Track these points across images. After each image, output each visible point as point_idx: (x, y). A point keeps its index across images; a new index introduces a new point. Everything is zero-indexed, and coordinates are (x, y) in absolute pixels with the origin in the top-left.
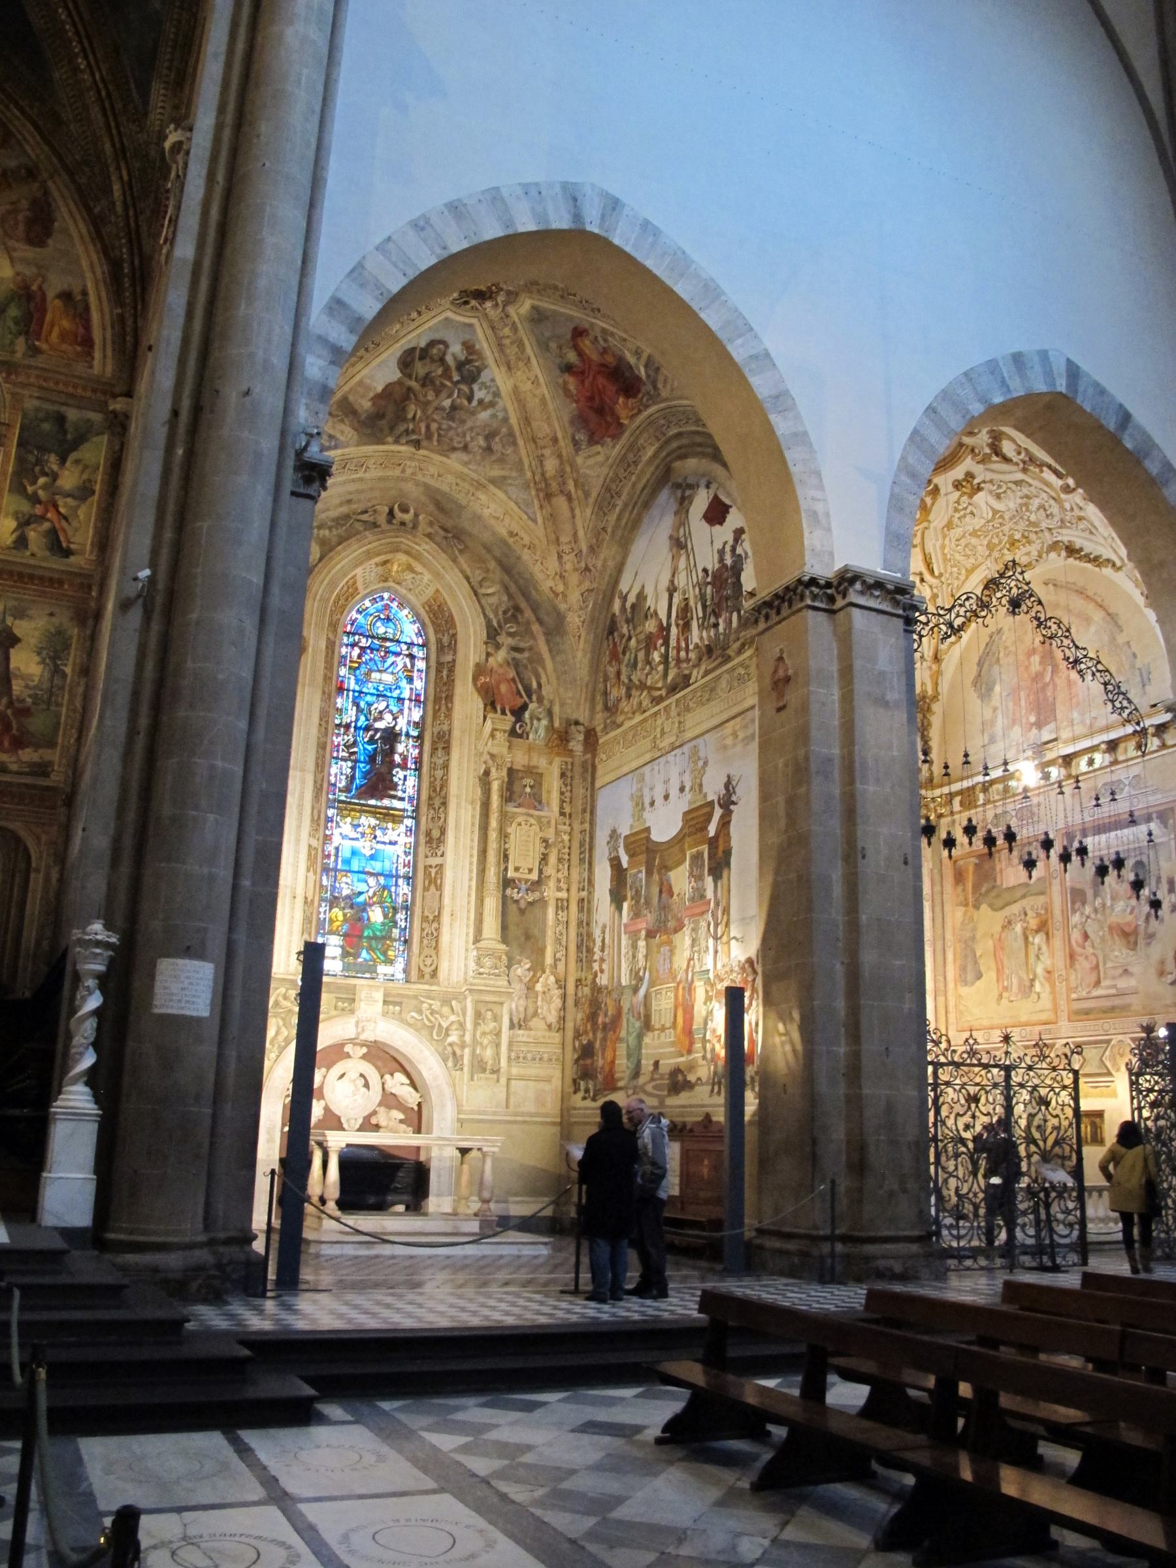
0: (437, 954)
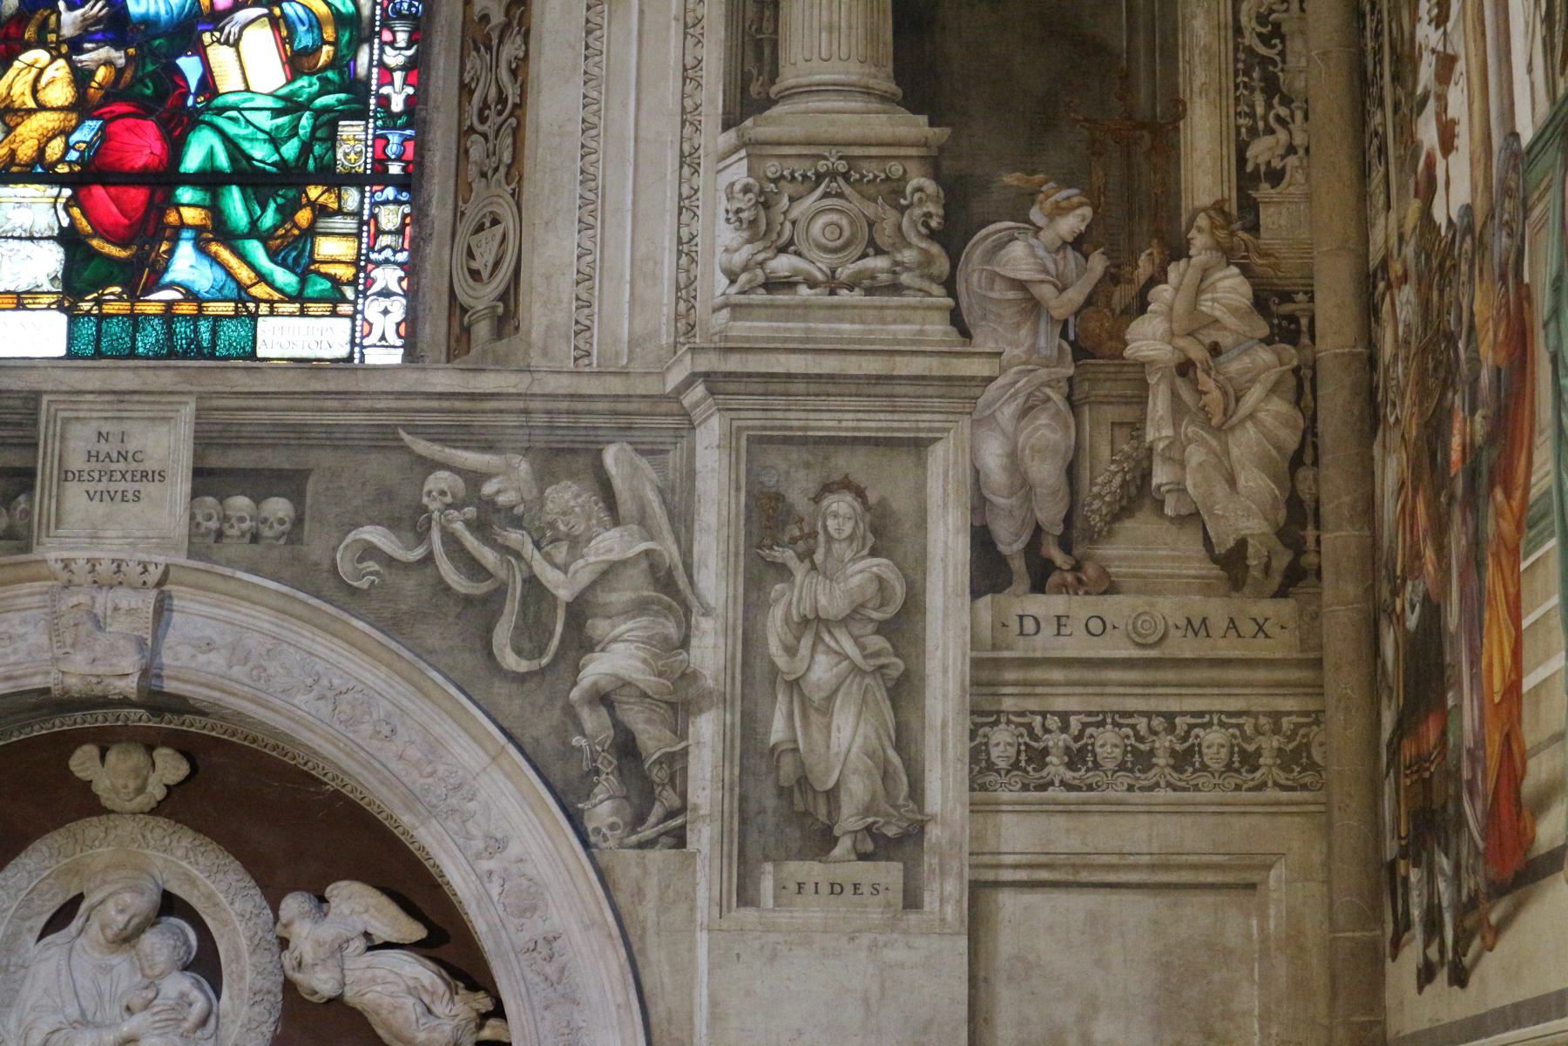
0: (516, 195)
